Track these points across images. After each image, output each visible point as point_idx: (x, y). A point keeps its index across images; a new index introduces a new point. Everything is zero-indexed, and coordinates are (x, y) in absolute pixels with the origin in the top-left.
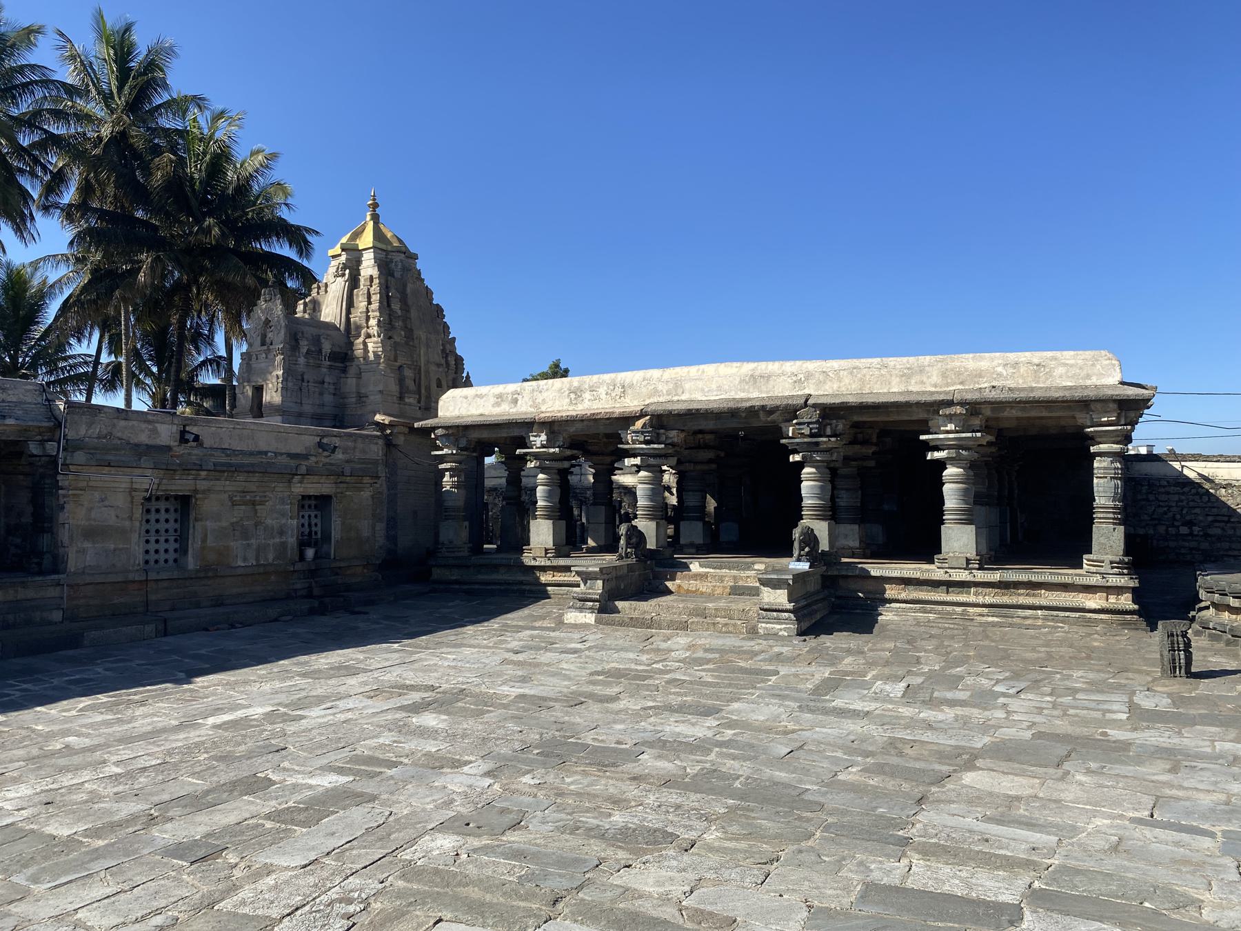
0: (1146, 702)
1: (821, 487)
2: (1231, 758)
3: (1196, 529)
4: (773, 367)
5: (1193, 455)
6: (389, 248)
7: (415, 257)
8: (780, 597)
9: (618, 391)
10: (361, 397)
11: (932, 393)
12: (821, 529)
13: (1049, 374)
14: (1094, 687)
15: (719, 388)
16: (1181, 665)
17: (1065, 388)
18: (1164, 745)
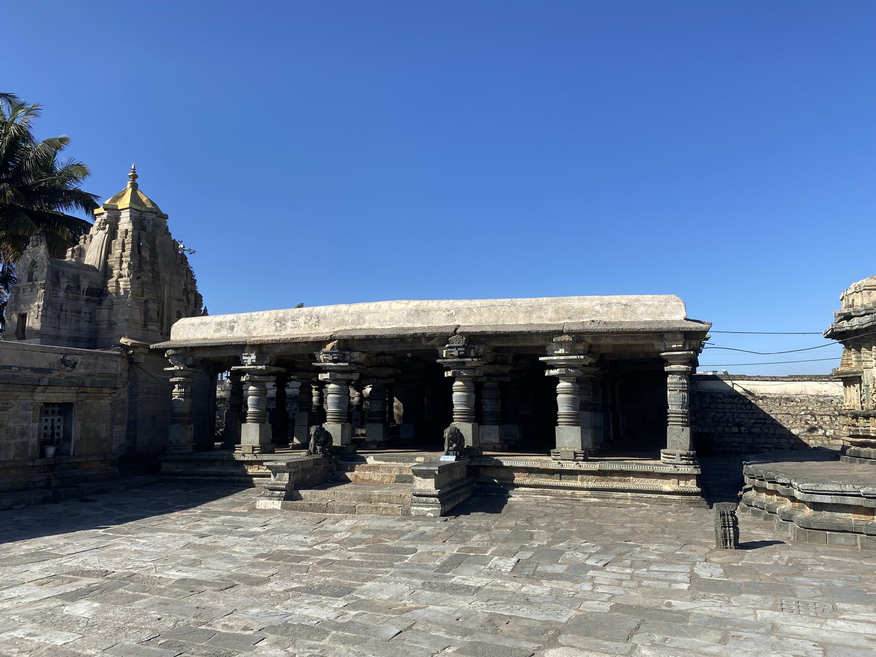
0: (704, 572)
1: (467, 397)
2: (770, 627)
3: (743, 428)
4: (432, 304)
5: (740, 376)
6: (144, 209)
7: (166, 217)
8: (428, 485)
9: (314, 320)
10: (111, 324)
11: (548, 325)
12: (467, 430)
13: (634, 312)
14: (667, 559)
15: (392, 319)
16: (732, 539)
17: (646, 322)
18: (717, 615)
